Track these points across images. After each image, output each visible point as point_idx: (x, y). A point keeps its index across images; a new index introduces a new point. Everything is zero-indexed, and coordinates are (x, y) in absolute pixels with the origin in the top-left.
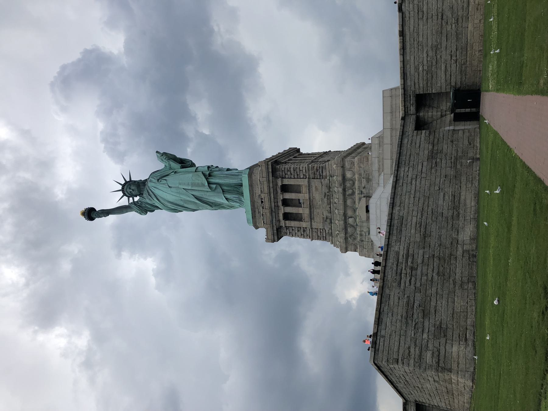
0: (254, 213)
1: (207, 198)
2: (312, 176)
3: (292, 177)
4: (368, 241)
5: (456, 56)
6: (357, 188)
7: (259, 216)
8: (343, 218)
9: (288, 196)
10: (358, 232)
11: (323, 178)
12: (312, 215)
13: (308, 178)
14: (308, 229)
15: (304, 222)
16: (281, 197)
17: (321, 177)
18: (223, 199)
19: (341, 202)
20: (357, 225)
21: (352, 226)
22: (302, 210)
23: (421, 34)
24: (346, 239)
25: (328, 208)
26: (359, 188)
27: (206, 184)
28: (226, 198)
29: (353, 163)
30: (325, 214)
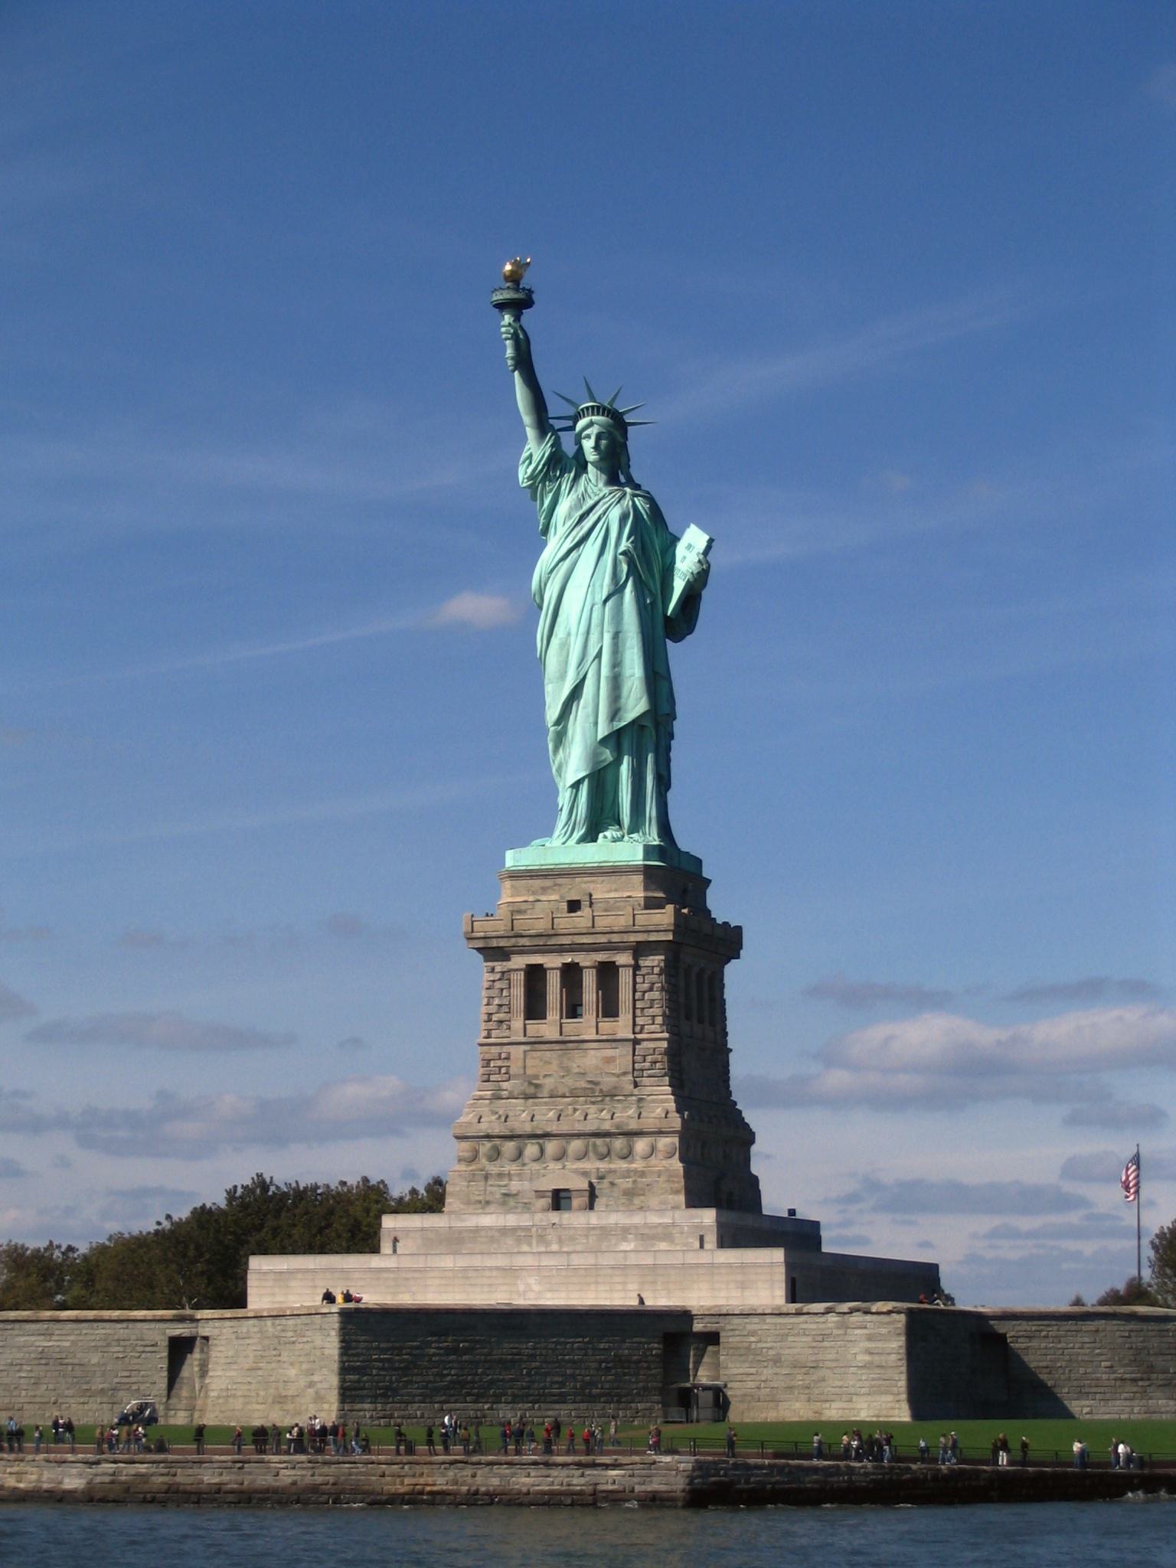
3: (638, 995)
4: (487, 1192)
5: (765, 1388)
6: (612, 1166)
7: (533, 889)
8: (539, 1132)
14: (507, 1033)
15: (525, 1025)
16: (585, 960)
18: (577, 770)
19: (580, 1127)
20: (524, 1165)
21: (520, 1154)
22: (555, 1021)
23: (796, 1339)
24: (488, 1137)
26: (611, 1171)
29: (670, 1157)
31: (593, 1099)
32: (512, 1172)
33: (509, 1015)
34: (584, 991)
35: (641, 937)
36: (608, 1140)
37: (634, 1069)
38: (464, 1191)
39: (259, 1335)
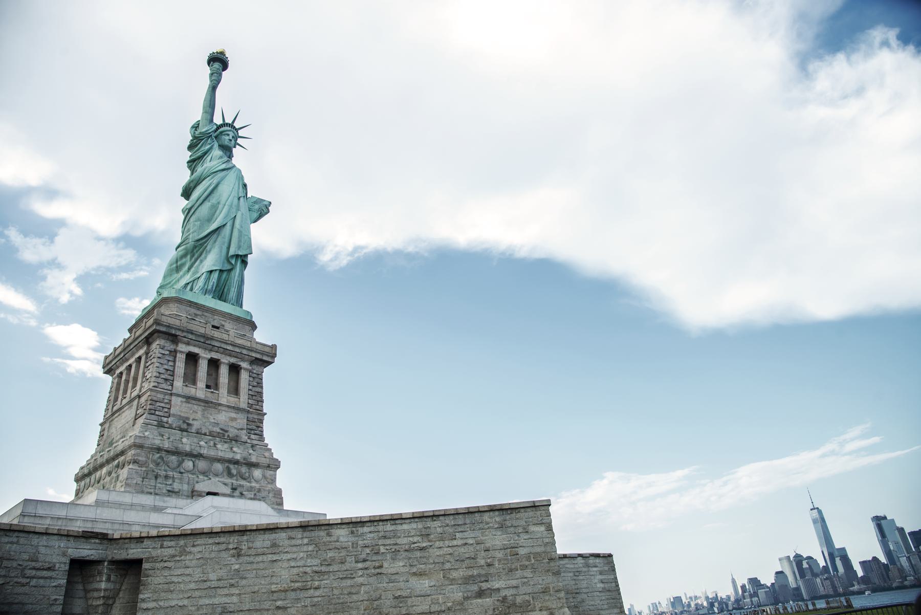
0: (197, 307)
1: (217, 243)
2: (250, 416)
4: (157, 487)
8: (195, 453)
9: (224, 371)
10: (171, 473)
11: (249, 433)
12: (194, 402)
13: (249, 410)
14: (170, 388)
17: (249, 430)
18: (214, 265)
19: (220, 454)
21: (179, 466)
22: (203, 388)
24: (159, 449)
25: (206, 431)
26: (241, 486)
27: (240, 253)
28: (214, 272)
30: (195, 423)
31: (225, 440)
32: (175, 476)
33: (172, 378)
34: (221, 376)
35: (258, 356)
36: (236, 466)
37: (247, 429)
38: (139, 484)
39: (311, 548)
